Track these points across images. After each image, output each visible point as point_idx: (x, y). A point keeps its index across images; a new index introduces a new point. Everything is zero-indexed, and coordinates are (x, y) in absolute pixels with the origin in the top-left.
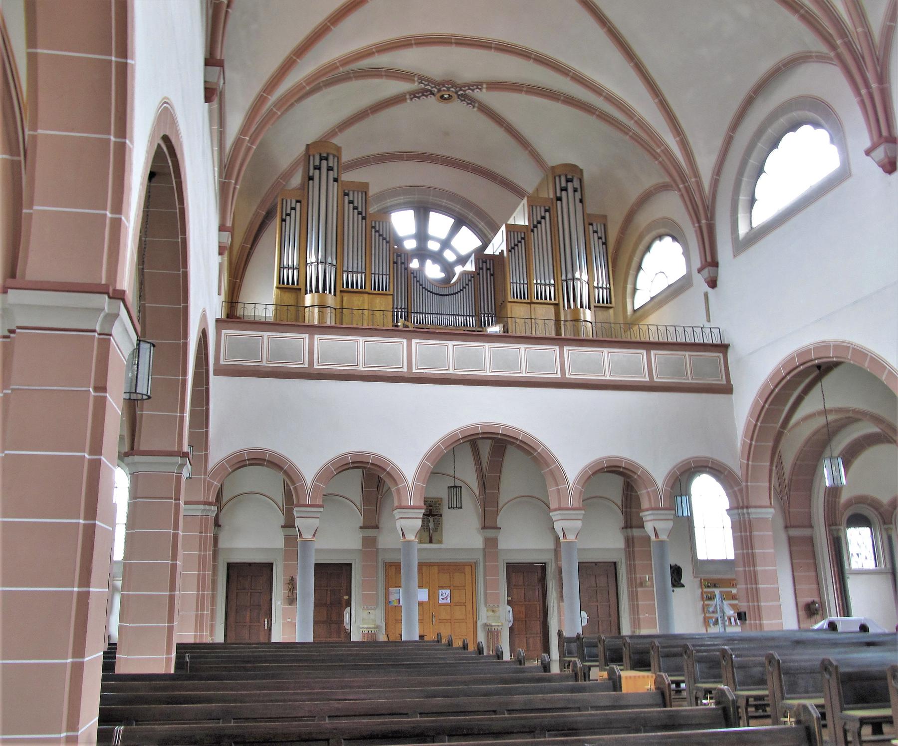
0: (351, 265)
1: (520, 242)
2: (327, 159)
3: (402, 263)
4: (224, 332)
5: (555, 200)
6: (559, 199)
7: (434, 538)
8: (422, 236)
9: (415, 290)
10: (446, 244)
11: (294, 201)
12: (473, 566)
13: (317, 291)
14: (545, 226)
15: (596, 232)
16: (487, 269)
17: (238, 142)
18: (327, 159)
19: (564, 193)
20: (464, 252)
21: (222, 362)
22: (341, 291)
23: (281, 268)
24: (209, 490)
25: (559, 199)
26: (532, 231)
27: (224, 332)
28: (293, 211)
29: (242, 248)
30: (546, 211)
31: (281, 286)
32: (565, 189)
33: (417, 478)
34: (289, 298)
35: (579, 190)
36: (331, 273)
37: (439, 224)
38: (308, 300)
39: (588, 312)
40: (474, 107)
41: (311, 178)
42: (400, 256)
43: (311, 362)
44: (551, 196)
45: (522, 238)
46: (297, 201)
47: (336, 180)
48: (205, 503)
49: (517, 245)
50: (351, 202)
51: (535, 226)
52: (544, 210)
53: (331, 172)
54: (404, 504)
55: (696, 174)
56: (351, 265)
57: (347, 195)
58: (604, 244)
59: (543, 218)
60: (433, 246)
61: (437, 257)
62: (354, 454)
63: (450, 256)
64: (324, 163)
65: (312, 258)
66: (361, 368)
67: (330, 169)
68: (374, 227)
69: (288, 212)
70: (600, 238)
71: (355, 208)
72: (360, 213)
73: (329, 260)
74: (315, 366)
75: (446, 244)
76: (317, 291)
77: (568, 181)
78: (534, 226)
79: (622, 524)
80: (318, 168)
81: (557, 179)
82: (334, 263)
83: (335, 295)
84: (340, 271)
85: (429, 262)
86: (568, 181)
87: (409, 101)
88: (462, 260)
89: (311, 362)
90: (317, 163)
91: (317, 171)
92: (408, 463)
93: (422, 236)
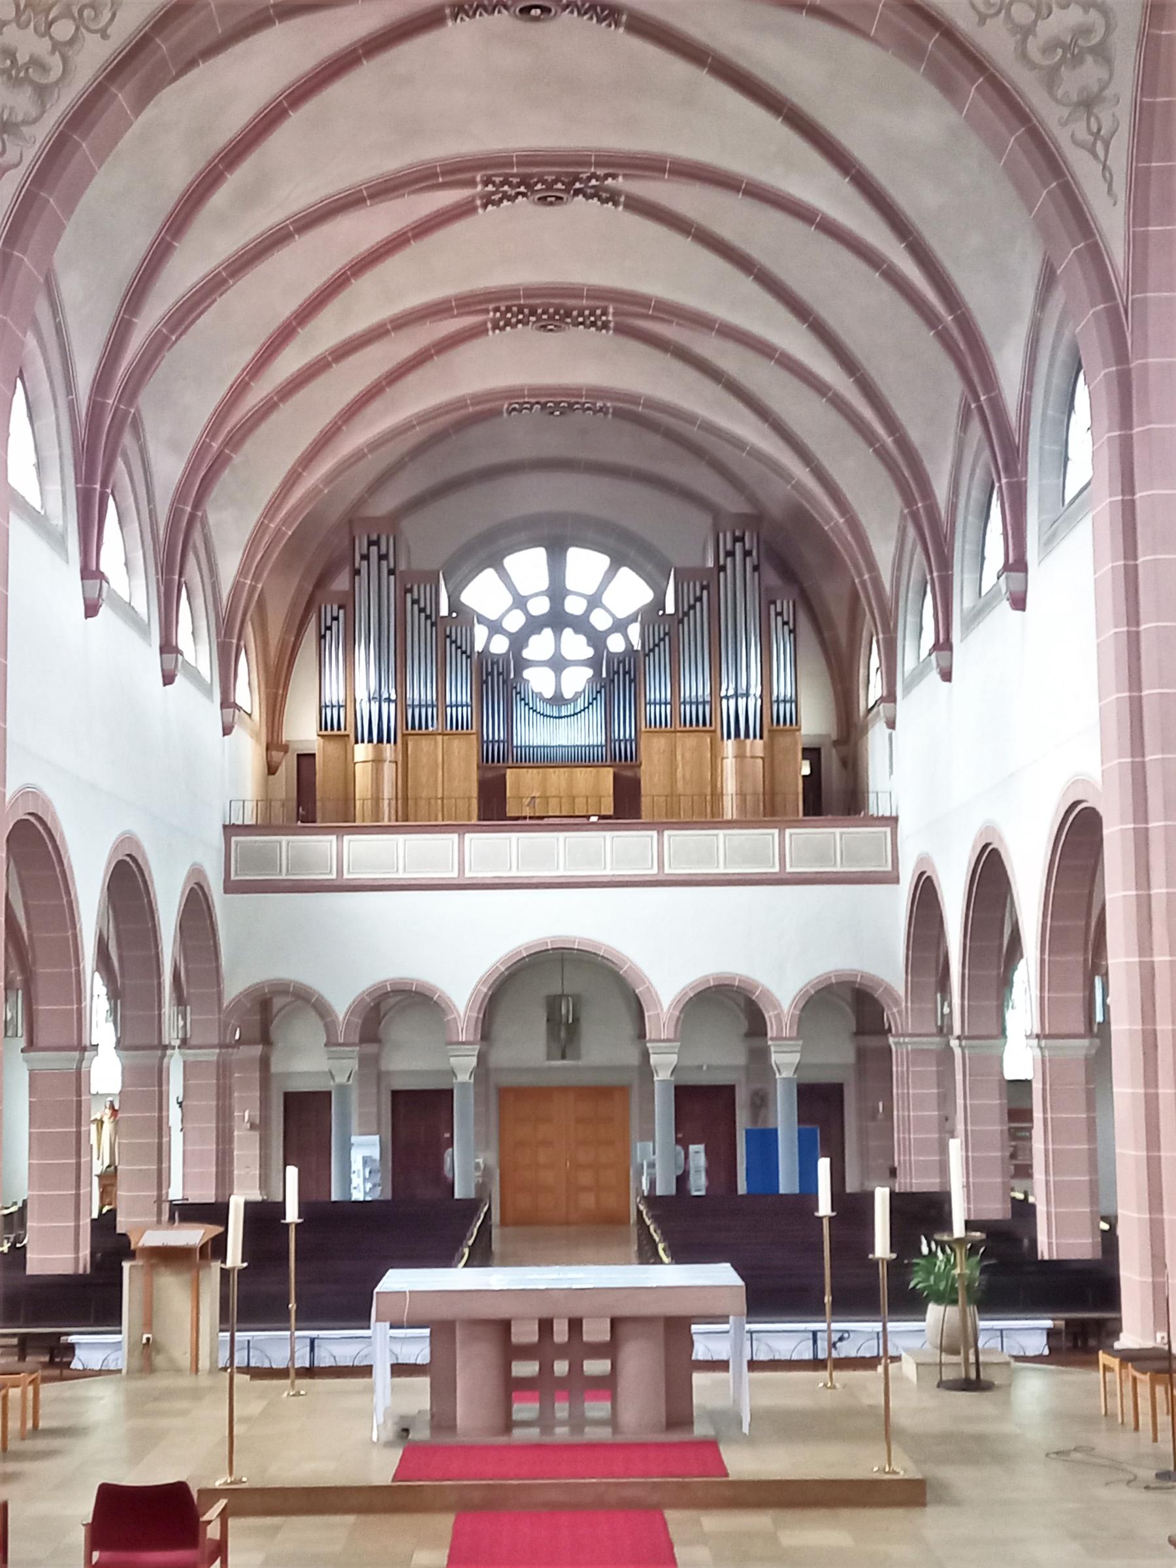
0: (416, 696)
1: (663, 639)
2: (377, 543)
3: (499, 674)
4: (234, 839)
5: (716, 573)
6: (723, 568)
7: (567, 1051)
8: (557, 592)
9: (520, 710)
10: (594, 601)
11: (335, 607)
12: (624, 1090)
13: (371, 741)
14: (701, 612)
15: (781, 614)
16: (625, 673)
17: (237, 587)
18: (377, 543)
19: (729, 559)
20: (622, 614)
21: (233, 877)
22: (404, 735)
23: (322, 708)
24: (225, 1030)
25: (723, 568)
26: (681, 621)
27: (234, 839)
28: (335, 623)
29: (283, 643)
30: (703, 588)
31: (323, 733)
32: (731, 554)
33: (469, 1008)
34: (334, 748)
35: (755, 553)
36: (389, 710)
37: (585, 566)
38: (362, 752)
39: (758, 741)
40: (606, 414)
41: (357, 572)
42: (498, 663)
43: (340, 871)
44: (710, 564)
45: (665, 634)
46: (340, 608)
47: (391, 572)
48: (221, 1046)
49: (658, 645)
50: (414, 602)
51: (686, 614)
52: (701, 587)
53: (384, 563)
54: (454, 1039)
55: (872, 566)
56: (416, 696)
57: (411, 590)
58: (790, 632)
59: (700, 599)
60: (575, 606)
61: (581, 625)
62: (394, 983)
63: (601, 621)
64: (374, 549)
65: (361, 694)
66: (401, 875)
67: (382, 557)
68: (450, 636)
69: (329, 624)
70: (785, 623)
71: (421, 610)
72: (428, 617)
73: (385, 695)
74: (346, 876)
75: (594, 601)
76: (371, 741)
77: (736, 540)
78: (680, 617)
79: (854, 1029)
80: (365, 557)
81: (721, 536)
82: (393, 697)
83: (395, 742)
84: (402, 703)
85: (568, 632)
86: (736, 540)
87: (505, 415)
88: (620, 626)
89: (340, 871)
90: (365, 551)
91: (365, 563)
92: (461, 986)
93: (557, 592)
